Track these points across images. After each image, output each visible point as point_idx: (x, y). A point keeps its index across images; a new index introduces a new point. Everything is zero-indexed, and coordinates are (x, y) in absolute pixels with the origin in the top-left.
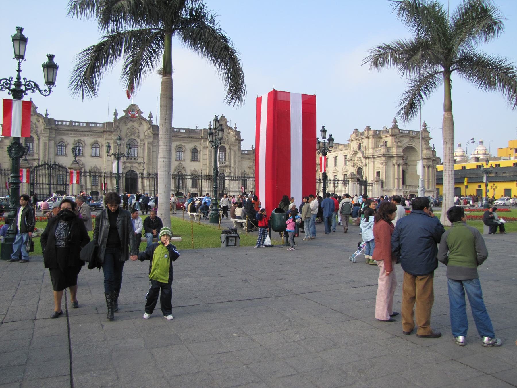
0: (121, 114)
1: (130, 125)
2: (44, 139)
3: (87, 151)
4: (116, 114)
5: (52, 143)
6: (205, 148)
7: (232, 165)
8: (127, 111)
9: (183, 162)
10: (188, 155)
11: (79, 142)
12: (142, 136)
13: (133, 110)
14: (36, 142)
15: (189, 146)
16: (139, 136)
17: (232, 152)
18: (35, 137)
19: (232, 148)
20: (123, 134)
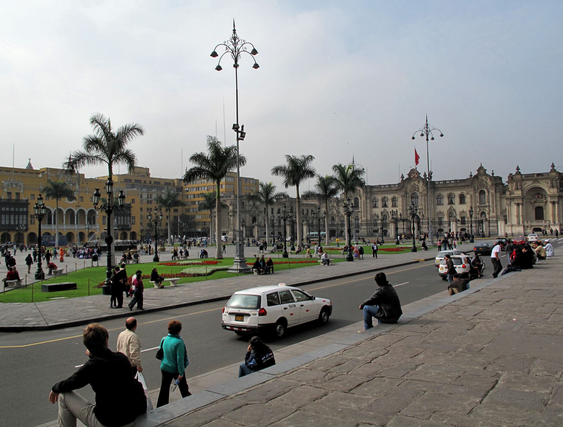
0: (406, 177)
1: (412, 183)
2: (363, 199)
3: (390, 203)
4: (402, 177)
5: (368, 201)
6: (468, 193)
7: (491, 205)
8: (409, 175)
9: (453, 206)
10: (457, 200)
11: (384, 198)
12: (421, 191)
13: (414, 173)
14: (360, 201)
15: (457, 193)
16: (418, 191)
17: (490, 194)
18: (359, 198)
19: (490, 191)
20: (408, 190)
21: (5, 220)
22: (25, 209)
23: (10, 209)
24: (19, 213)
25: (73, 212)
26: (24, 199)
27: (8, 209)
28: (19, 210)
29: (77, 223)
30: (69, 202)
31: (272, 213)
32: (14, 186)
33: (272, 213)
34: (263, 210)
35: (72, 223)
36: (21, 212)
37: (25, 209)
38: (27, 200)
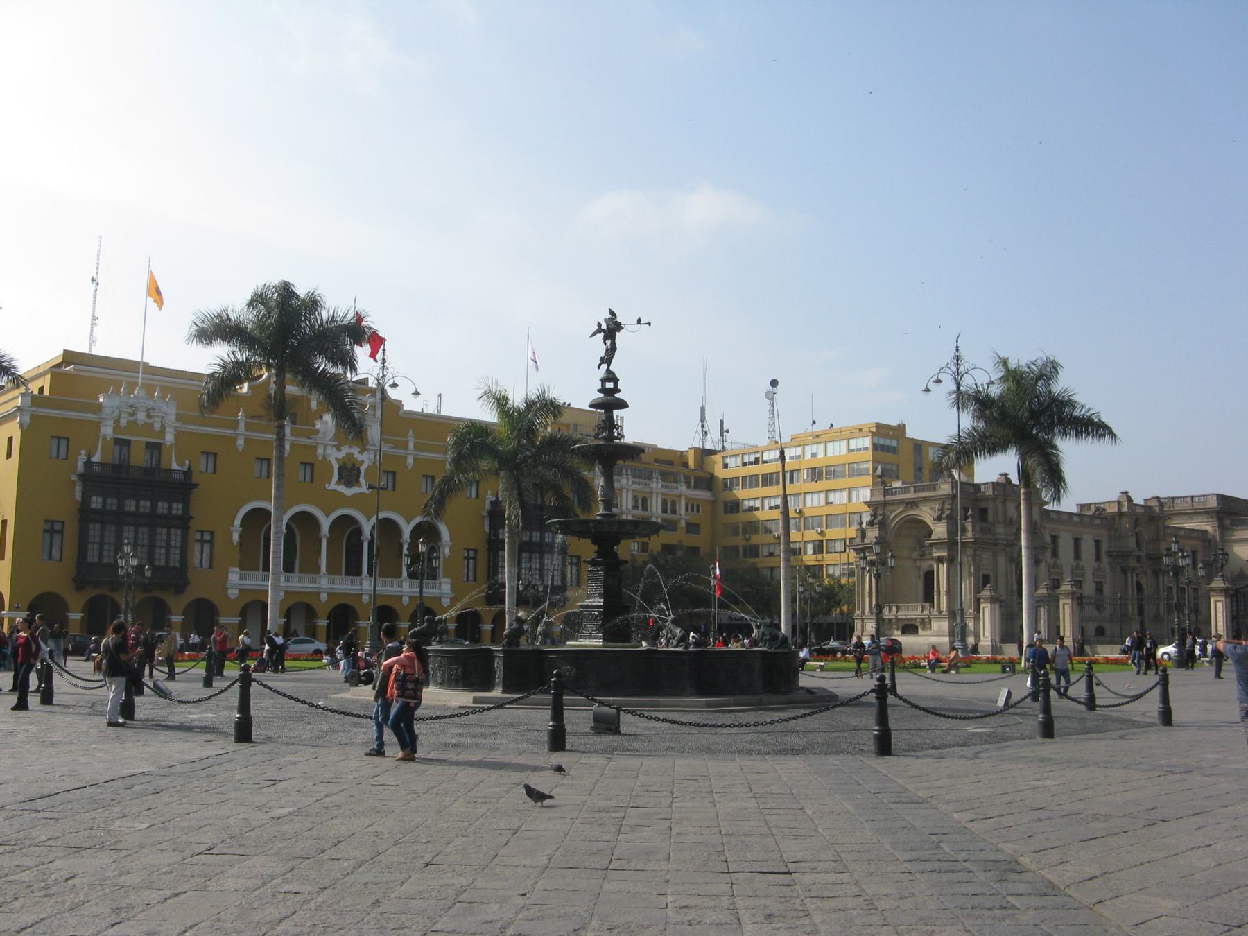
21: (101, 544)
22: (177, 508)
23: (121, 505)
24: (152, 521)
25: (359, 531)
26: (175, 466)
27: (112, 504)
29: (370, 573)
30: (342, 489)
31: (1077, 556)
32: (141, 417)
33: (1077, 556)
34: (1049, 540)
35: (353, 569)
36: (161, 516)
37: (177, 508)
38: (188, 474)
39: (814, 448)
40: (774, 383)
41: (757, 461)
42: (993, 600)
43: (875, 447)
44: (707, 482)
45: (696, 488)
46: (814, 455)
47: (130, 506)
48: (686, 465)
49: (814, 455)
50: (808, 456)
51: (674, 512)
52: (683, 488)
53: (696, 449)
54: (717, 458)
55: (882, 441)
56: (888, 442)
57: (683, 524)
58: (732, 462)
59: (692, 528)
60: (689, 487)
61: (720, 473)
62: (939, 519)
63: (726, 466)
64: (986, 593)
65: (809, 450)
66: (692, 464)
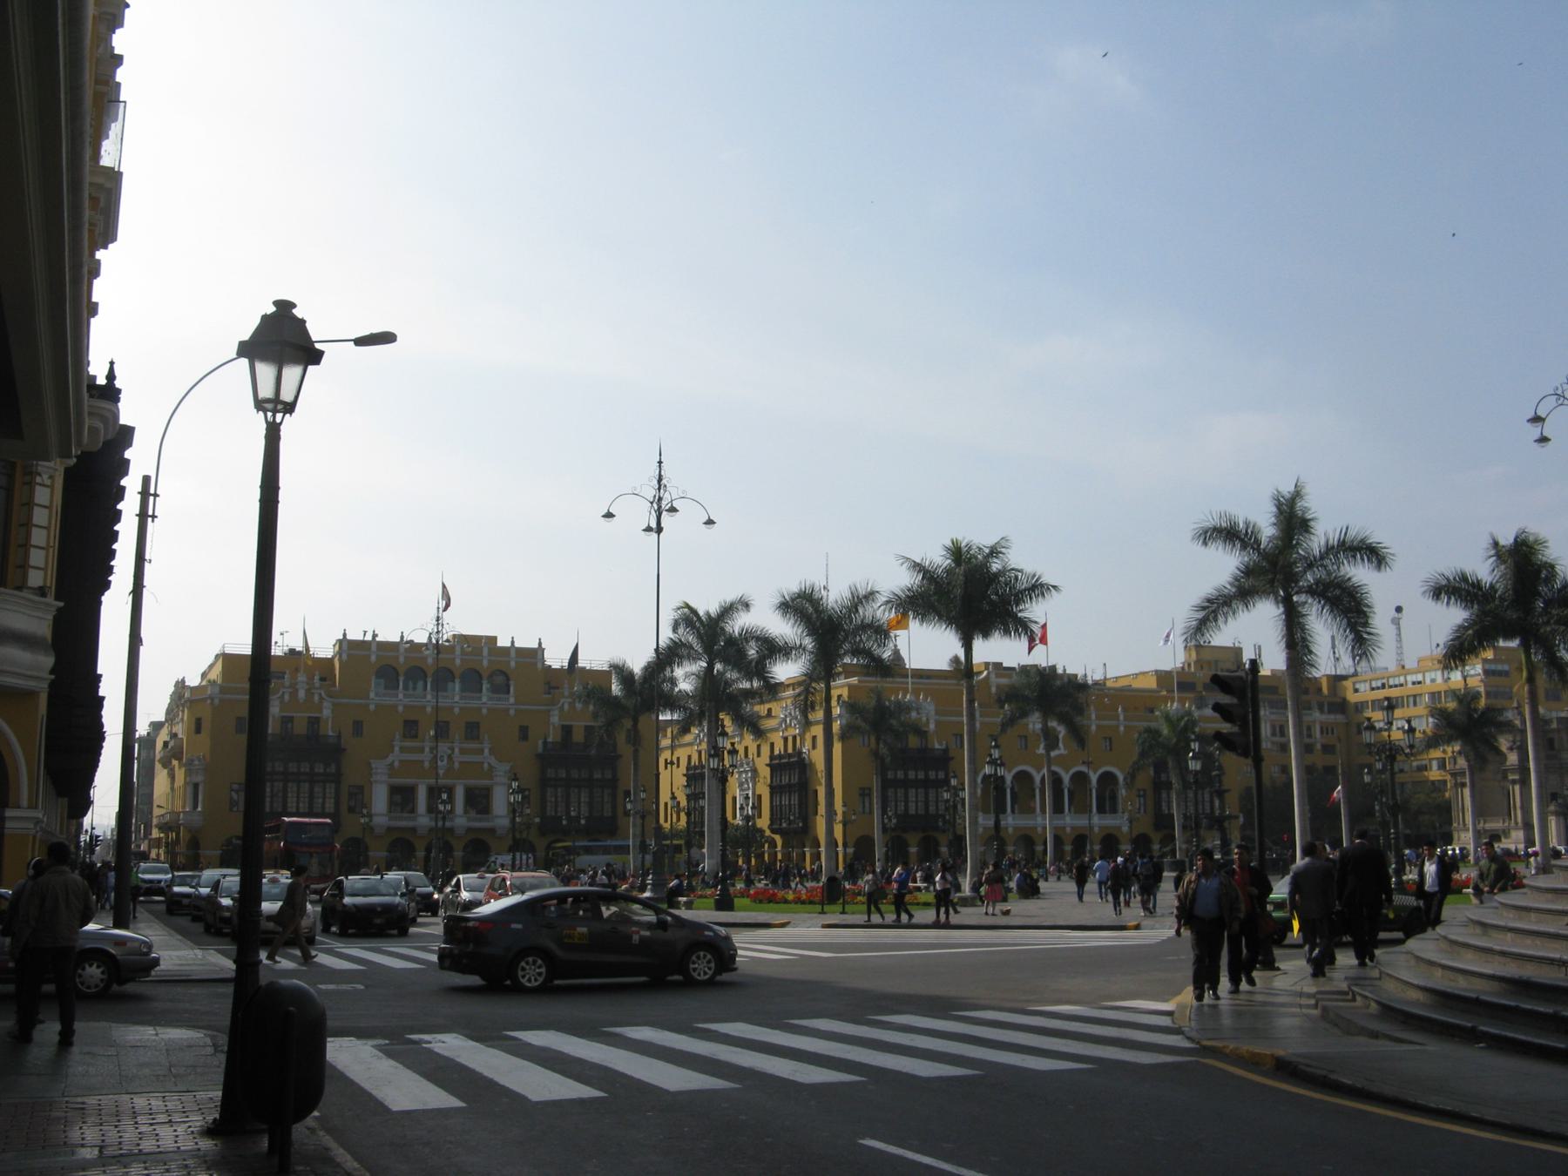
24: (926, 784)
26: (937, 746)
28: (927, 775)
38: (946, 751)
39: (1433, 675)
40: (1399, 609)
41: (1383, 686)
42: (1557, 814)
43: (1486, 672)
44: (1341, 706)
45: (1330, 712)
46: (1433, 681)
47: (912, 774)
48: (1320, 689)
49: (1433, 681)
50: (1428, 681)
51: (1310, 736)
52: (1317, 715)
53: (1328, 676)
54: (1348, 684)
55: (1493, 667)
56: (1499, 667)
57: (1319, 746)
58: (1361, 687)
59: (1328, 749)
60: (1322, 711)
61: (1352, 698)
62: (1511, 749)
63: (1356, 691)
64: (1552, 808)
65: (1428, 676)
66: (1325, 690)
